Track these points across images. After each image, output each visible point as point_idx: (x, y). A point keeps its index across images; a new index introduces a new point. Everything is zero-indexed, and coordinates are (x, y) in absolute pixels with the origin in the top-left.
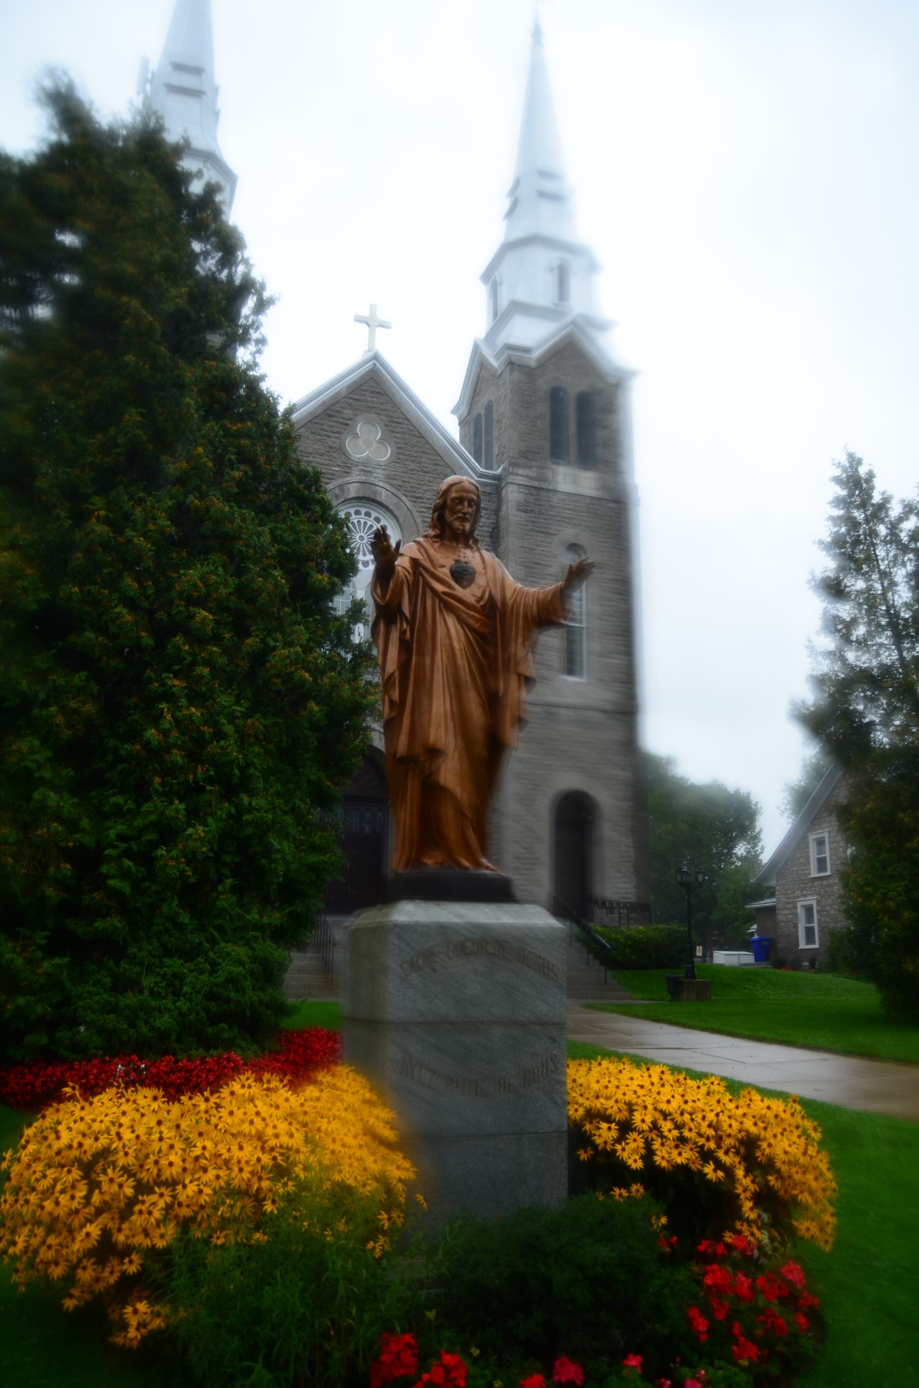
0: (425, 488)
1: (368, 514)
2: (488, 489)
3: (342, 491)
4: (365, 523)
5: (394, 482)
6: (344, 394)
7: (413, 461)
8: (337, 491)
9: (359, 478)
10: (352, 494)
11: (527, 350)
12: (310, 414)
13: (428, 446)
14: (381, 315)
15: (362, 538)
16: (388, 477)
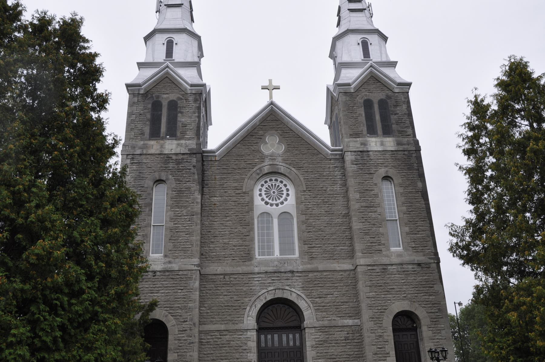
0: (304, 162)
1: (276, 180)
2: (338, 157)
3: (261, 171)
4: (275, 185)
5: (287, 162)
6: (258, 124)
7: (296, 150)
8: (258, 171)
9: (269, 163)
10: (266, 172)
11: (349, 85)
12: (242, 136)
13: (303, 141)
14: (274, 84)
15: (274, 192)
16: (284, 160)
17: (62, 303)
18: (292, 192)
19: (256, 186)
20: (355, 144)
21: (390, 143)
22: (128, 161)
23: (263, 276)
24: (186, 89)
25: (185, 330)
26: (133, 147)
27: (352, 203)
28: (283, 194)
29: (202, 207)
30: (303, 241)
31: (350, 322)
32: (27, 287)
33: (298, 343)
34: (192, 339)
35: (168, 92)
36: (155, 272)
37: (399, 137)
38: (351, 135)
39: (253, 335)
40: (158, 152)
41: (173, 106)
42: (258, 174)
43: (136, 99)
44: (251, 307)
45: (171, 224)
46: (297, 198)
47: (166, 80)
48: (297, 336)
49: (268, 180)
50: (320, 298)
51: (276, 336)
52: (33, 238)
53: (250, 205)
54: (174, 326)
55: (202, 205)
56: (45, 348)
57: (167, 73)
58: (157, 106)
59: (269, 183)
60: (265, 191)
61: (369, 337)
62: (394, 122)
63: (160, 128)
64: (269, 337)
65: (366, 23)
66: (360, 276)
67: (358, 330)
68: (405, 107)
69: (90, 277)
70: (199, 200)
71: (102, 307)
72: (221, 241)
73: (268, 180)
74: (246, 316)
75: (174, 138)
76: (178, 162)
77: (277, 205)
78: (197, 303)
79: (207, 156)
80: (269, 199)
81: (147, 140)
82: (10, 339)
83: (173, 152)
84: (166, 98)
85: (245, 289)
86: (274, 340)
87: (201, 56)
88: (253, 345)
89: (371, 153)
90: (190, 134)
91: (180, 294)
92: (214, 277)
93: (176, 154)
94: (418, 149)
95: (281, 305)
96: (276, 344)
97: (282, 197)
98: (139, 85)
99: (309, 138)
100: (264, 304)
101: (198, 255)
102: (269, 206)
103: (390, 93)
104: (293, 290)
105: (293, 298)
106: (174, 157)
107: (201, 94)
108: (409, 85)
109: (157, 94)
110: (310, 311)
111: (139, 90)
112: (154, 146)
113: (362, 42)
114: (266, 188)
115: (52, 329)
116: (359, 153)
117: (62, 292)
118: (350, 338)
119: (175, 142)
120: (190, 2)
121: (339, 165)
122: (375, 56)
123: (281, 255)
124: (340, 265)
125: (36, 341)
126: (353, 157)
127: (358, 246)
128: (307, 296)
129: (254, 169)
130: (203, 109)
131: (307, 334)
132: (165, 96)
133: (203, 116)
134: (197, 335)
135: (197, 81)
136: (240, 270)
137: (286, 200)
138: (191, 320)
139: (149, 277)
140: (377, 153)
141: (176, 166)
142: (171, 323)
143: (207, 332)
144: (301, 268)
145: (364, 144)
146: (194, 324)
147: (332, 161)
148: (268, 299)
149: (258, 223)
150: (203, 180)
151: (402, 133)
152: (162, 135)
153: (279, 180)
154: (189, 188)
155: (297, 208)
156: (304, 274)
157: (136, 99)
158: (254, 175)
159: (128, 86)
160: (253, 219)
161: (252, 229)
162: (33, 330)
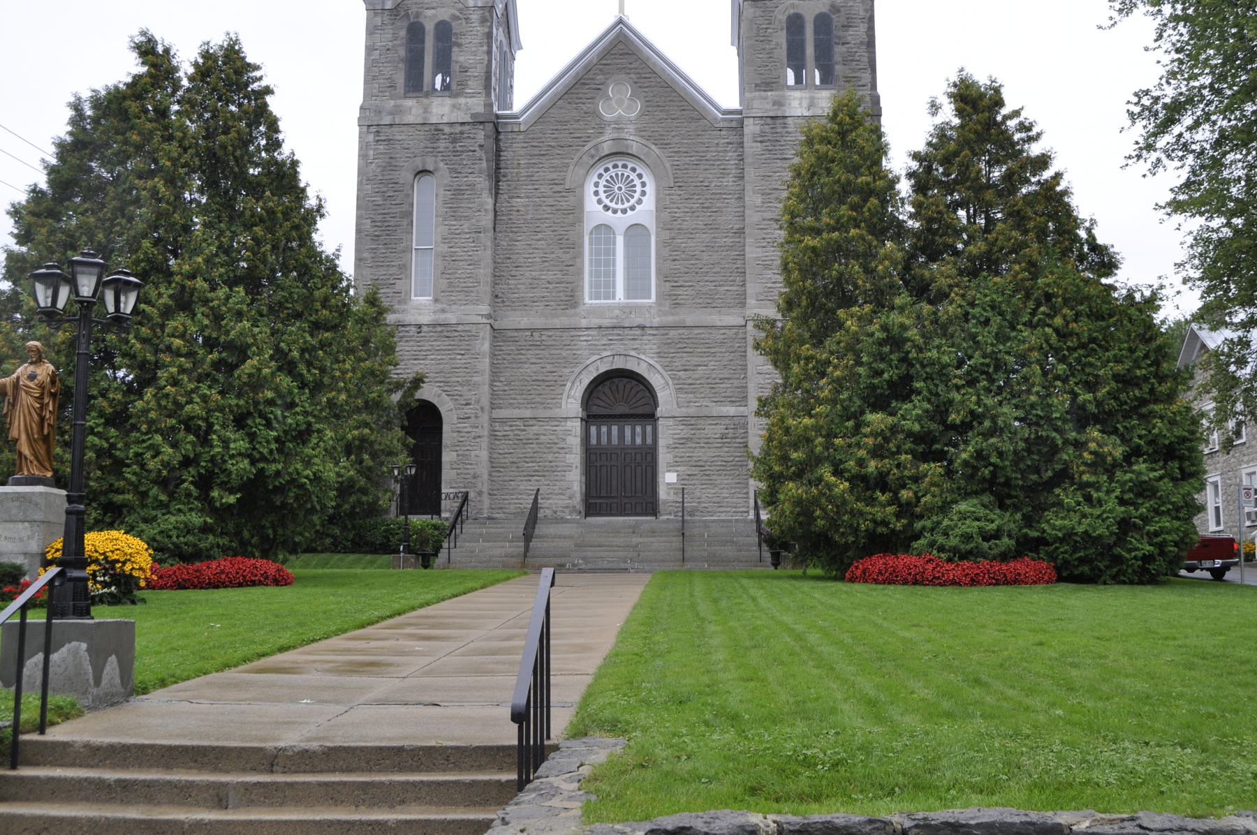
1: (625, 166)
2: (734, 124)
3: (597, 150)
8: (593, 151)
9: (611, 136)
10: (607, 152)
15: (620, 189)
16: (639, 130)
17: (276, 418)
18: (650, 189)
20: (763, 104)
22: (371, 137)
23: (594, 333)
26: (378, 112)
27: (747, 212)
29: (495, 216)
30: (664, 277)
31: (731, 410)
32: (242, 402)
33: (649, 441)
34: (479, 431)
36: (420, 326)
38: (757, 85)
39: (576, 426)
40: (419, 121)
41: (444, 31)
42: (592, 157)
43: (378, 20)
45: (444, 248)
46: (658, 200)
48: (649, 428)
49: (610, 166)
51: (615, 429)
52: (244, 357)
53: (576, 212)
55: (495, 211)
56: (263, 459)
58: (415, 32)
59: (612, 172)
62: (840, 59)
63: (421, 74)
64: (604, 429)
67: (740, 424)
68: (863, 28)
69: (303, 386)
70: (490, 206)
71: (314, 416)
73: (610, 166)
74: (565, 396)
75: (447, 93)
77: (624, 211)
78: (487, 376)
79: (506, 124)
81: (400, 98)
82: (232, 452)
83: (445, 120)
86: (609, 434)
88: (575, 441)
89: (789, 121)
90: (474, 85)
91: (460, 361)
94: (877, 115)
95: (626, 380)
96: (615, 441)
97: (632, 197)
101: (488, 298)
104: (642, 357)
105: (641, 369)
106: (447, 130)
109: (414, 9)
110: (668, 392)
112: (413, 110)
115: (268, 442)
116: (769, 121)
117: (276, 405)
119: (448, 101)
121: (735, 139)
124: (723, 317)
125: (255, 453)
126: (758, 128)
127: (752, 289)
128: (664, 367)
129: (586, 148)
130: (499, 34)
131: (660, 428)
132: (429, 13)
133: (500, 47)
134: (486, 425)
136: (556, 322)
137: (640, 202)
138: (478, 402)
141: (451, 146)
142: (446, 407)
143: (503, 421)
144: (656, 321)
145: (779, 103)
146: (482, 408)
147: (723, 133)
148: (602, 370)
149: (591, 244)
150: (498, 168)
152: (425, 89)
153: (630, 165)
154: (472, 186)
155: (658, 218)
156: (662, 331)
157: (378, 20)
158: (585, 158)
161: (580, 255)
162: (251, 442)
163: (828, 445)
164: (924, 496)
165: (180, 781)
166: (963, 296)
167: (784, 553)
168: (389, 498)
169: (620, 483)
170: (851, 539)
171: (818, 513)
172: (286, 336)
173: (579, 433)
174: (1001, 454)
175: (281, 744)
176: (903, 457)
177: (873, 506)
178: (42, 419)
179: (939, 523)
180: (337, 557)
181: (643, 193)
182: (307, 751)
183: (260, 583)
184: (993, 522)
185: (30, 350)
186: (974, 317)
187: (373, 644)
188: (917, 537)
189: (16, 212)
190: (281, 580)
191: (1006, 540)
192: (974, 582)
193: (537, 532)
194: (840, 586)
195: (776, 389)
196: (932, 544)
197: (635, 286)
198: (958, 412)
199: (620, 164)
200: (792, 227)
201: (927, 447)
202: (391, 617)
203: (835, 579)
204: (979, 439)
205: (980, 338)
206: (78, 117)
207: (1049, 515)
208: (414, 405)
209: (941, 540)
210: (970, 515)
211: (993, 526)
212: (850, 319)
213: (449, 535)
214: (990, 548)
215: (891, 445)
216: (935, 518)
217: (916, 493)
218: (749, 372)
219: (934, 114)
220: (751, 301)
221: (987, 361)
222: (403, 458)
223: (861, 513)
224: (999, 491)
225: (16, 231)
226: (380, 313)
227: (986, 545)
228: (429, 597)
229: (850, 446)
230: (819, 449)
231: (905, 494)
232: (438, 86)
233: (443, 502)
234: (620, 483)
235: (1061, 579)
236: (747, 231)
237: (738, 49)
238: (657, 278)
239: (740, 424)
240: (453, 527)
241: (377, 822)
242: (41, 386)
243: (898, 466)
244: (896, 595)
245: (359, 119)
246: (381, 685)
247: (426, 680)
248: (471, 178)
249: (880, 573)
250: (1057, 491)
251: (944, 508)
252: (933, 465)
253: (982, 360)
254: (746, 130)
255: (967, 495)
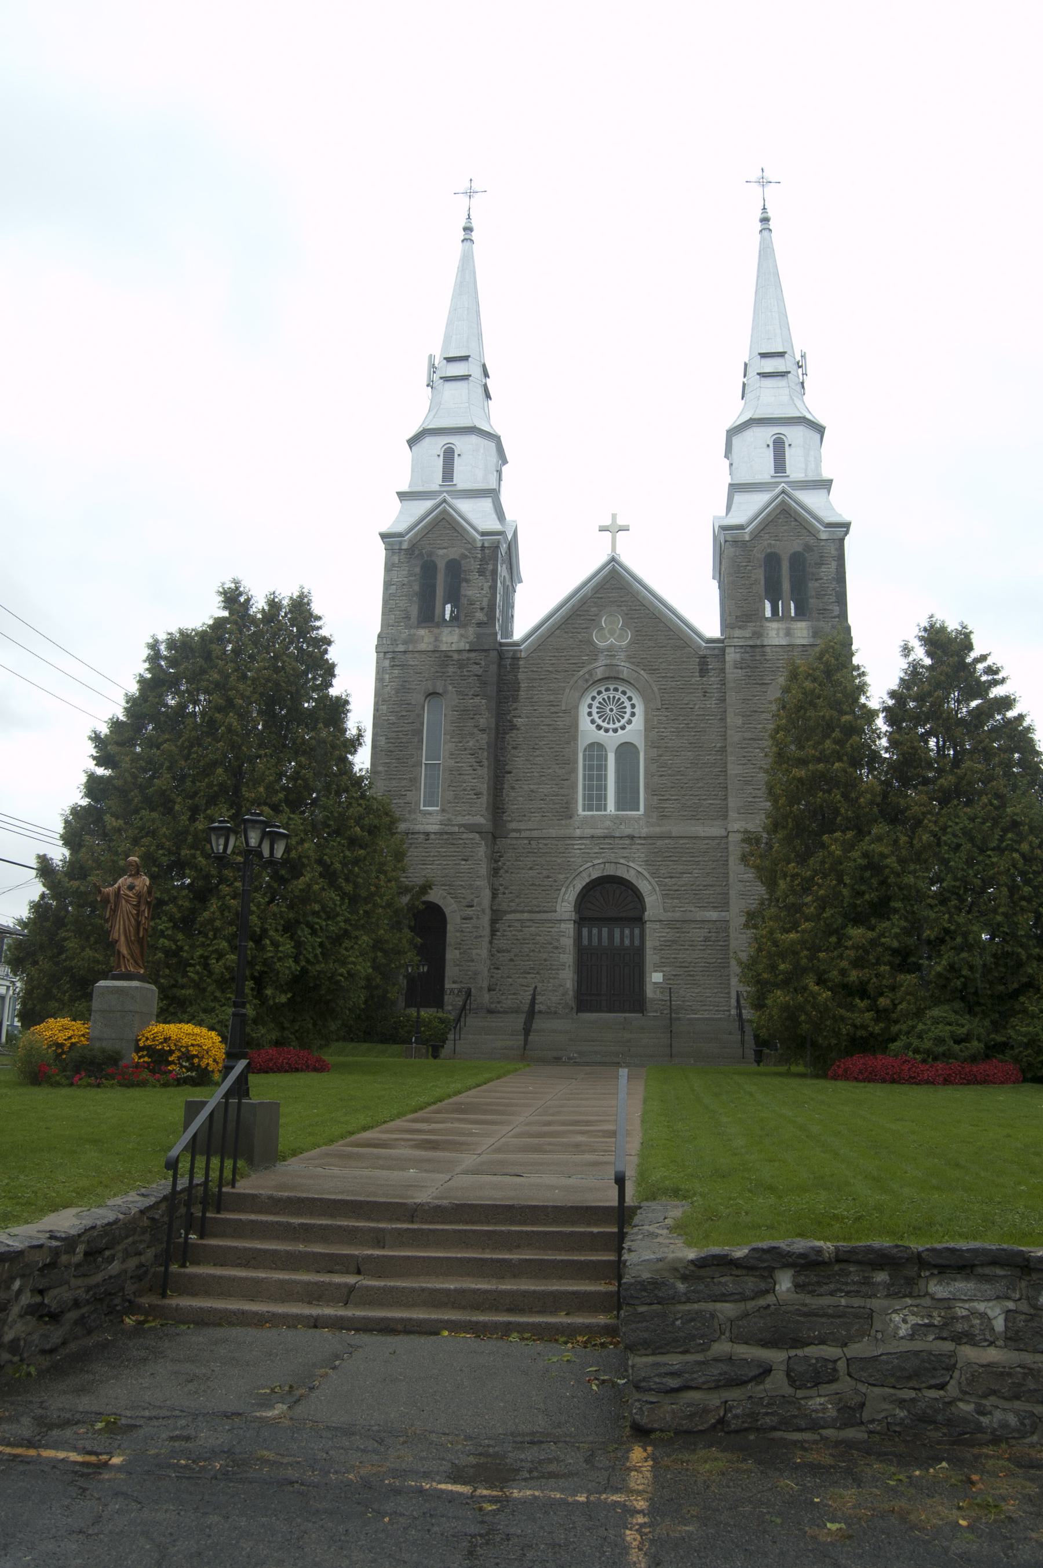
1: (616, 690)
2: (716, 652)
3: (591, 675)
4: (614, 697)
6: (590, 595)
8: (587, 676)
10: (600, 677)
11: (741, 527)
14: (620, 522)
15: (611, 710)
16: (629, 657)
18: (639, 710)
19: (583, 700)
21: (802, 632)
22: (387, 663)
23: (588, 842)
24: (474, 540)
25: (471, 918)
27: (729, 732)
28: (625, 713)
30: (651, 791)
31: (714, 915)
33: (637, 943)
35: (446, 545)
36: (427, 834)
37: (818, 620)
39: (569, 928)
40: (431, 648)
41: (455, 569)
42: (587, 681)
44: (567, 888)
45: (451, 763)
46: (647, 721)
47: (442, 525)
48: (637, 931)
49: (603, 689)
50: (671, 877)
51: (605, 930)
54: (455, 911)
57: (445, 511)
59: (605, 695)
60: (598, 708)
61: (737, 939)
62: (813, 593)
64: (595, 931)
65: (785, 399)
66: (731, 848)
67: (723, 927)
68: (834, 564)
70: (493, 726)
72: (526, 787)
73: (603, 689)
74: (559, 900)
76: (461, 665)
77: (615, 731)
79: (508, 651)
80: (604, 721)
84: (443, 555)
85: (559, 861)
86: (600, 935)
87: (500, 479)
88: (568, 942)
89: (768, 649)
92: (515, 842)
93: (459, 651)
96: (605, 942)
97: (623, 718)
98: (400, 535)
99: (671, 620)
100: (588, 884)
102: (602, 732)
103: (811, 541)
104: (631, 864)
105: (630, 876)
106: (456, 656)
107: (498, 547)
108: (846, 526)
110: (655, 897)
111: (401, 543)
112: (425, 639)
113: (775, 442)
114: (600, 703)
118: (713, 939)
119: (457, 630)
120: (484, 366)
122: (795, 470)
123: (618, 809)
126: (738, 655)
127: (732, 803)
128: (652, 874)
129: (581, 673)
130: (502, 570)
131: (648, 931)
132: (441, 552)
133: (504, 583)
135: (494, 525)
136: (553, 832)
137: (629, 722)
139: (420, 841)
140: (778, 649)
144: (645, 831)
145: (757, 634)
146: (483, 911)
148: (594, 877)
149: (584, 760)
151: (823, 612)
152: (436, 620)
153: (621, 689)
155: (646, 737)
157: (396, 559)
159: (384, 536)
160: (576, 754)
161: (574, 770)
163: (812, 958)
164: (900, 1003)
165: (348, 1226)
166: (935, 822)
167: (766, 1051)
168: (397, 992)
169: (609, 980)
170: (834, 1041)
171: (803, 1018)
172: (327, 851)
173: (572, 933)
174: (971, 968)
175: (418, 1201)
176: (882, 968)
177: (853, 1012)
178: (138, 923)
179: (914, 1027)
180: (352, 1045)
181: (633, 714)
182: (440, 1206)
183: (302, 1070)
184: (963, 1026)
185: (130, 864)
186: (946, 844)
187: (434, 1126)
188: (894, 1040)
189: (96, 738)
190: (321, 1067)
191: (975, 1043)
192: (947, 1081)
193: (534, 1026)
194: (822, 1083)
195: (762, 904)
196: (908, 1046)
197: (627, 798)
198: (932, 928)
199: (612, 687)
200: (781, 757)
201: (904, 960)
202: (434, 1103)
203: (817, 1076)
204: (952, 953)
205: (952, 863)
206: (154, 658)
207: (1014, 1021)
208: (422, 907)
209: (916, 1043)
210: (941, 1022)
211: (964, 1030)
212: (834, 844)
213: (455, 1028)
214: (961, 1051)
215: (871, 957)
216: (910, 1023)
217: (892, 1001)
218: (731, 880)
219: (906, 656)
220: (732, 814)
221: (958, 884)
222: (411, 955)
223: (843, 1019)
224: (969, 1001)
225: (95, 754)
226: (393, 823)
227: (956, 1047)
228: (459, 1086)
229: (832, 959)
230: (804, 961)
231: (883, 1002)
232: (447, 617)
233: (446, 997)
234: (609, 980)
235: (1025, 1080)
236: (729, 749)
237: (719, 582)
238: (646, 792)
239: (723, 927)
240: (459, 1020)
241: (504, 1260)
242: (139, 896)
243: (877, 975)
244: (876, 1092)
245: (377, 647)
246: (469, 1160)
247: (500, 1156)
248: (477, 700)
249: (860, 1072)
250: (1022, 999)
251: (919, 1014)
252: (908, 977)
253: (953, 883)
254: (728, 658)
255: (937, 1002)
